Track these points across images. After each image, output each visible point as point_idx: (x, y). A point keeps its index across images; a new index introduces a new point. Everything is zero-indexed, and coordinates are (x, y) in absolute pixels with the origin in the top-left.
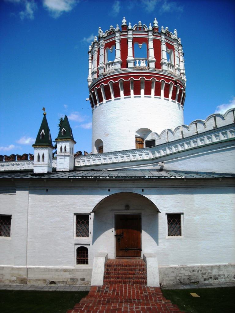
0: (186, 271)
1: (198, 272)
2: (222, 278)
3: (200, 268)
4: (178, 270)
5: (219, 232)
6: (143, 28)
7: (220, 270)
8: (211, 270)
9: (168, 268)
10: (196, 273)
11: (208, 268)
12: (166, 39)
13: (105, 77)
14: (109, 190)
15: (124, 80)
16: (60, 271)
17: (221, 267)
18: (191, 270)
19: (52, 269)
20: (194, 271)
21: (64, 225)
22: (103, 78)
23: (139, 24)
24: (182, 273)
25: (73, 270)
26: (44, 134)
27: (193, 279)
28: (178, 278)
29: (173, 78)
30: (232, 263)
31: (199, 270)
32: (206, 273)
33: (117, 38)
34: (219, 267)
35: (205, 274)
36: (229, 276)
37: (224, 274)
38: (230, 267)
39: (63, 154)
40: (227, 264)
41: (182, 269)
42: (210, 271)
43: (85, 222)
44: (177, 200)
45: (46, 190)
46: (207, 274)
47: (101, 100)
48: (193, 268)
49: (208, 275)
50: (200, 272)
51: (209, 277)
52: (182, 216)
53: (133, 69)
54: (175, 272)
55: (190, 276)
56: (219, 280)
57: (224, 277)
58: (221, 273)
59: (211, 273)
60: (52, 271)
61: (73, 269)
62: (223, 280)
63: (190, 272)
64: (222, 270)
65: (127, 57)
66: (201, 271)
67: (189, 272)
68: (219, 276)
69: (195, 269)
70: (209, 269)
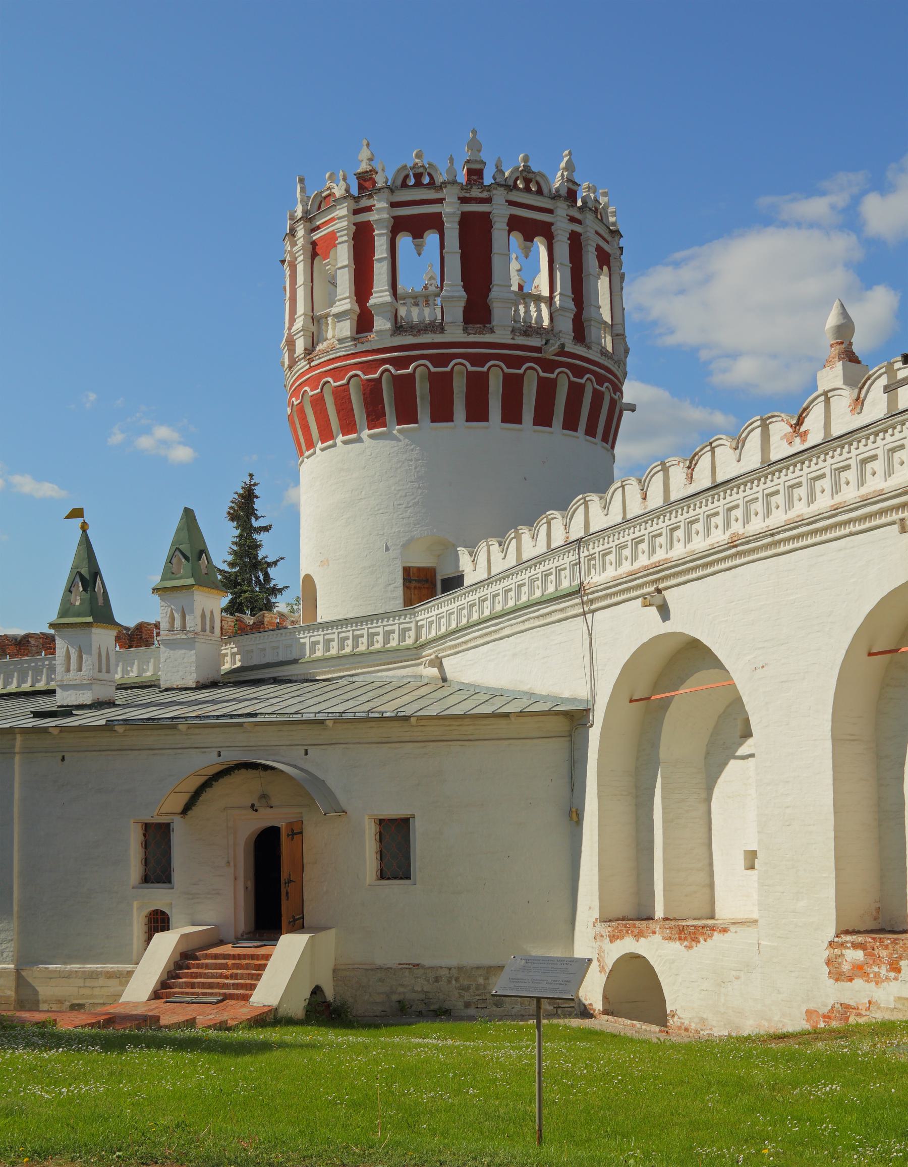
0: (418, 977)
1: (449, 982)
3: (454, 972)
8: (487, 979)
12: (511, 203)
13: (313, 364)
20: (437, 979)
22: (308, 367)
28: (395, 998)
31: (451, 978)
32: (472, 987)
42: (481, 980)
50: (454, 982)
51: (478, 998)
55: (427, 992)
59: (485, 988)
63: (428, 981)
66: (457, 979)
67: (426, 983)
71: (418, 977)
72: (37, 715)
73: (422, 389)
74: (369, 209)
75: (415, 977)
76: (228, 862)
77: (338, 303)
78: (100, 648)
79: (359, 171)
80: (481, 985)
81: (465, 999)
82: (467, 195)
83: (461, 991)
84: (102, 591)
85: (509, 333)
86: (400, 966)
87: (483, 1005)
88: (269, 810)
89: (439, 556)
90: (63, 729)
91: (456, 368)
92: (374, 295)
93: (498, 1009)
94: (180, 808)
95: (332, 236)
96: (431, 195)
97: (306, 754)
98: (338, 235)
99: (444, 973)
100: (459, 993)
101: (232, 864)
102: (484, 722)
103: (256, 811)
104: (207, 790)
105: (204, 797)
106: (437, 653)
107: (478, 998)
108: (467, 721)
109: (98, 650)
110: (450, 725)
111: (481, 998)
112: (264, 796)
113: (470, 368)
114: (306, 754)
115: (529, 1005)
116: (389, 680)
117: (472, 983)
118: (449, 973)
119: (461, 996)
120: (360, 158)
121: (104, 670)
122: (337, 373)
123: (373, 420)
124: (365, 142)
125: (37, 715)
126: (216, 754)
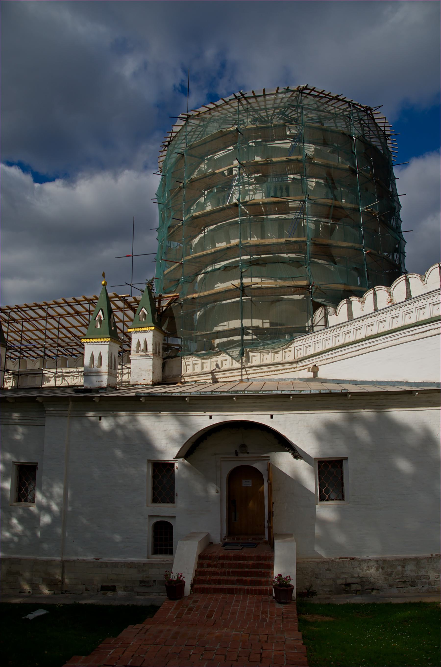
0: (355, 567)
4: (338, 565)
8: (403, 567)
14: (211, 418)
25: (144, 564)
26: (102, 319)
34: (417, 561)
35: (390, 574)
36: (437, 580)
51: (398, 580)
52: (344, 462)
56: (419, 586)
57: (427, 581)
59: (402, 574)
61: (145, 562)
68: (419, 578)
70: (399, 565)
71: (355, 567)
75: (353, 567)
86: (341, 560)
93: (413, 588)
100: (384, 577)
106: (315, 363)
107: (398, 580)
108: (382, 397)
117: (393, 570)
118: (377, 564)
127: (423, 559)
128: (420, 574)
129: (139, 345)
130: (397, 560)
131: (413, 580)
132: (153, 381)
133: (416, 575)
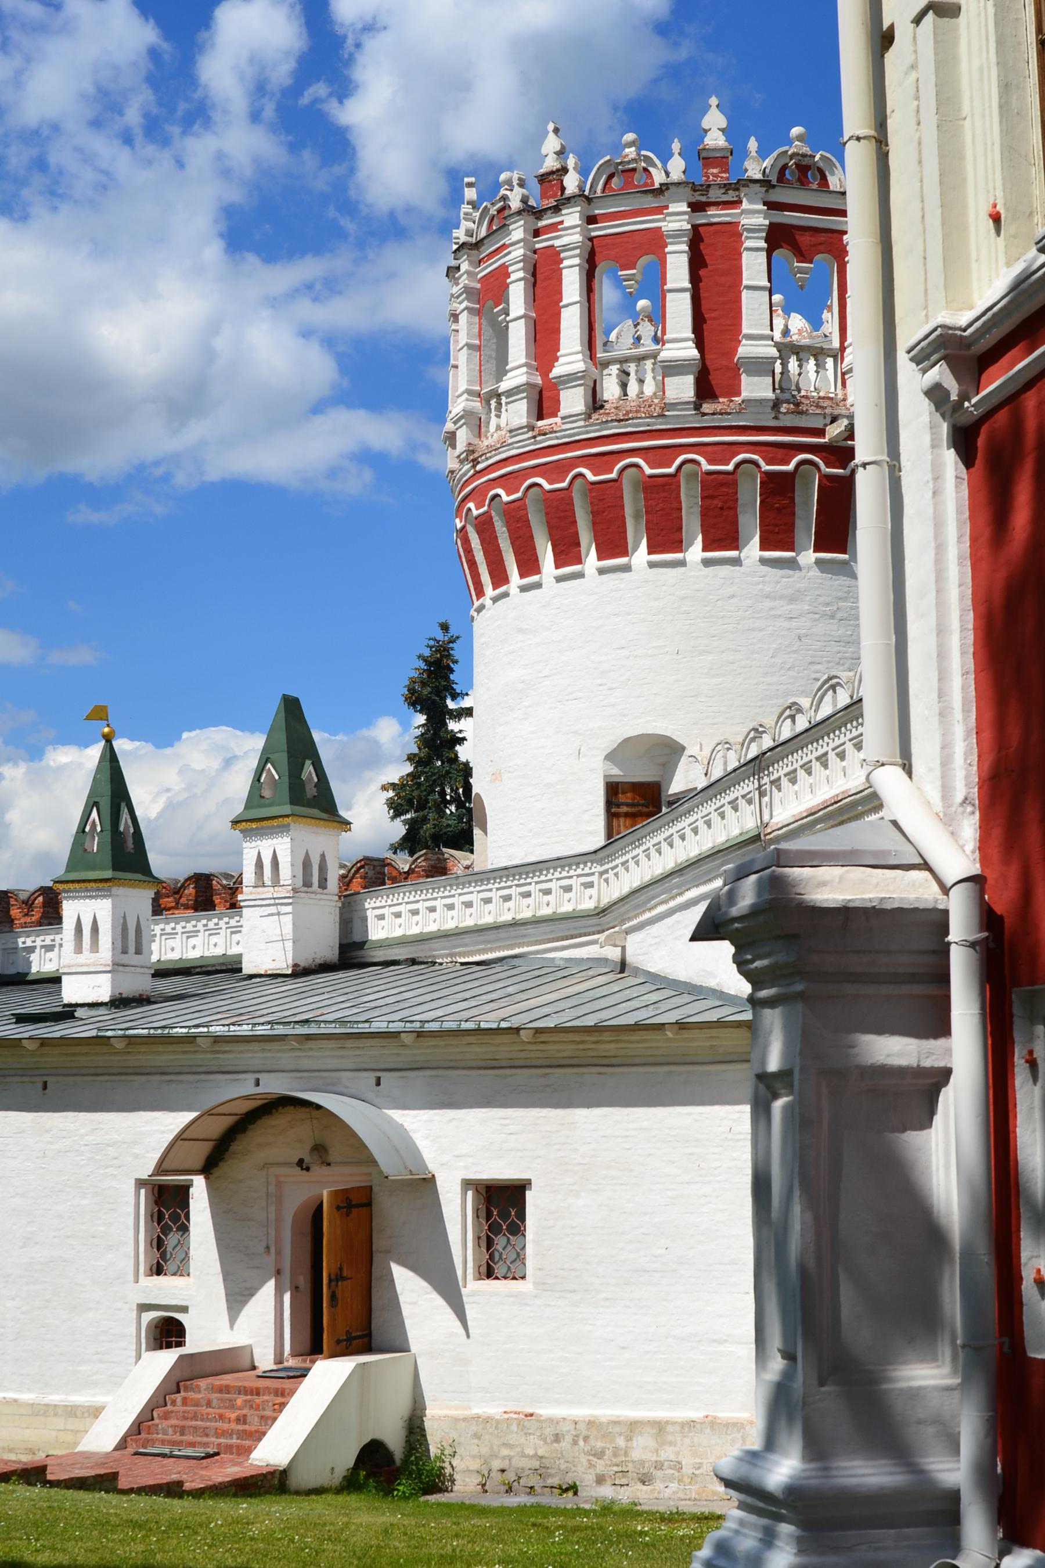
0: (530, 1434)
1: (575, 1442)
2: (672, 1478)
3: (582, 1427)
4: (496, 1428)
5: (675, 1271)
6: (645, 170)
7: (663, 1443)
8: (629, 1439)
9: (465, 1419)
10: (565, 1444)
11: (617, 1429)
13: (479, 467)
15: (547, 486)
16: (83, 1413)
17: (670, 1428)
18: (549, 1431)
19: (55, 1406)
21: (102, 1228)
22: (472, 472)
23: (627, 150)
24: (511, 1442)
27: (553, 1471)
29: (820, 432)
30: (719, 1415)
33: (513, 255)
34: (660, 1427)
35: (600, 1454)
36: (697, 1472)
37: (680, 1459)
38: (708, 1431)
39: (268, 892)
40: (697, 1415)
41: (514, 1428)
42: (621, 1442)
43: (183, 1216)
44: (508, 1121)
45: (40, 1085)
46: (609, 1453)
47: (500, 578)
48: (557, 1423)
49: (614, 1460)
50: (581, 1443)
51: (616, 1469)
53: (582, 423)
54: (487, 1437)
55: (541, 1457)
56: (659, 1486)
57: (676, 1474)
58: (667, 1454)
59: (626, 1454)
60: (55, 1415)
62: (674, 1486)
63: (545, 1441)
64: (671, 1444)
65: (557, 359)
66: (586, 1439)
67: (542, 1443)
68: (659, 1465)
69: (565, 1428)
71: (530, 1434)
72: (21, 1019)
73: (631, 505)
74: (553, 228)
75: (526, 1434)
76: (268, 1248)
77: (509, 375)
78: (124, 917)
79: (542, 171)
80: (621, 1449)
81: (598, 1471)
82: (703, 199)
83: (591, 1458)
84: (132, 830)
85: (769, 410)
86: (506, 1416)
87: (624, 1481)
88: (325, 1170)
89: (664, 765)
90: (44, 1042)
91: (687, 467)
92: (561, 360)
93: (645, 1488)
94: (199, 1162)
95: (503, 272)
96: (650, 202)
97: (378, 1084)
98: (511, 269)
99: (568, 1428)
100: (589, 1460)
101: (273, 1250)
102: (634, 1038)
103: (308, 1169)
104: (239, 1137)
105: (235, 1147)
108: (606, 1036)
109: (122, 921)
110: (582, 1042)
111: (620, 1469)
112: (319, 1149)
113: (706, 466)
114: (378, 1084)
115: (690, 1483)
116: (562, 963)
117: (608, 1445)
119: (591, 1466)
120: (544, 151)
121: (132, 949)
122: (509, 481)
123: (562, 552)
124: (551, 127)
125: (21, 1019)
126: (253, 1082)
127: (674, 1423)
128: (663, 1456)
129: (259, 864)
130: (616, 1423)
131: (645, 1471)
132: (295, 965)
133: (654, 1459)
